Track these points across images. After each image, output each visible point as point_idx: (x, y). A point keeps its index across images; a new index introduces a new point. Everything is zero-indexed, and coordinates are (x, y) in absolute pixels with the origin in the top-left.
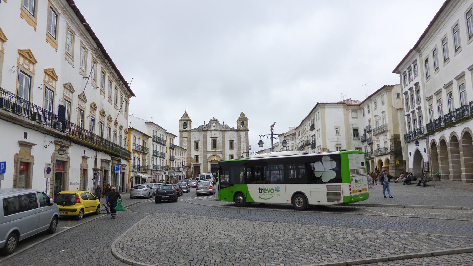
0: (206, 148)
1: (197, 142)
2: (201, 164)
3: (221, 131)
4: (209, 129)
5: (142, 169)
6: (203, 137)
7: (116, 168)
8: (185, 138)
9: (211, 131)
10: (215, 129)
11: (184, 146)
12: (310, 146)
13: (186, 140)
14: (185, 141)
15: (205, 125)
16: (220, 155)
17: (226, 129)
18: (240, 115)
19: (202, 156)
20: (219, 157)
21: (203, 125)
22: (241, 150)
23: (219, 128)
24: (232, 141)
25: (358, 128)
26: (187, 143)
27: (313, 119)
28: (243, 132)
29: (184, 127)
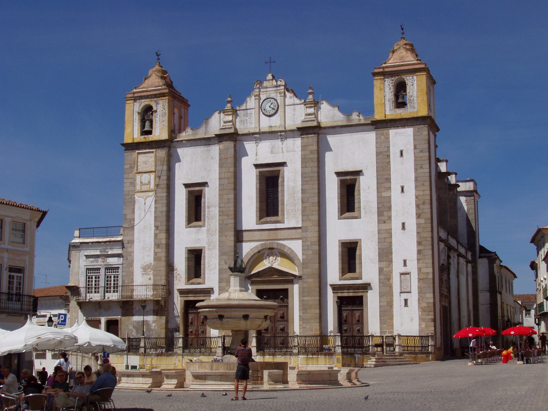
1: (197, 189)
5: (2, 309)
6: (221, 166)
13: (149, 182)
14: (145, 188)
19: (216, 252)
22: (390, 218)
24: (348, 177)
29: (143, 126)
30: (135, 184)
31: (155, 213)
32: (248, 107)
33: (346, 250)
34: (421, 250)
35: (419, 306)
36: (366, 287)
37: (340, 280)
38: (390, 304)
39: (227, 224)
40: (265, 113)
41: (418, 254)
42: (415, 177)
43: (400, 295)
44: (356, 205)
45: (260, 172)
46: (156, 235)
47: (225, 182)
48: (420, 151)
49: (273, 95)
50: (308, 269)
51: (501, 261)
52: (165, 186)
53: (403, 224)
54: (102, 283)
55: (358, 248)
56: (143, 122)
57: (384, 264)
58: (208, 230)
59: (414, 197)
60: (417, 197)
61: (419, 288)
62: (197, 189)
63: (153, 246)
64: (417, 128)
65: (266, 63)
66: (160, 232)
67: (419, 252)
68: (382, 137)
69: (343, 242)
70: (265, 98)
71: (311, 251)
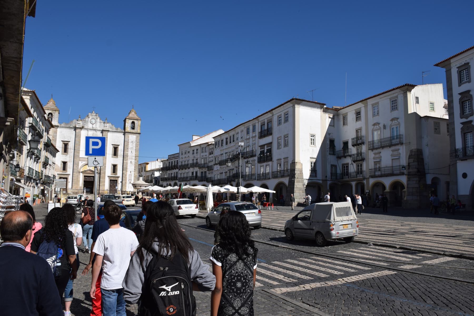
0: (79, 153)
2: (69, 175)
4: (86, 127)
7: (91, 147)
9: (87, 129)
10: (94, 127)
12: (256, 158)
17: (110, 130)
22: (127, 159)
23: (100, 127)
24: (116, 146)
25: (334, 139)
27: (267, 123)
28: (133, 136)
33: (113, 166)
36: (118, 177)
38: (126, 183)
49: (94, 118)
58: (69, 156)
60: (135, 154)
61: (134, 179)
67: (135, 169)
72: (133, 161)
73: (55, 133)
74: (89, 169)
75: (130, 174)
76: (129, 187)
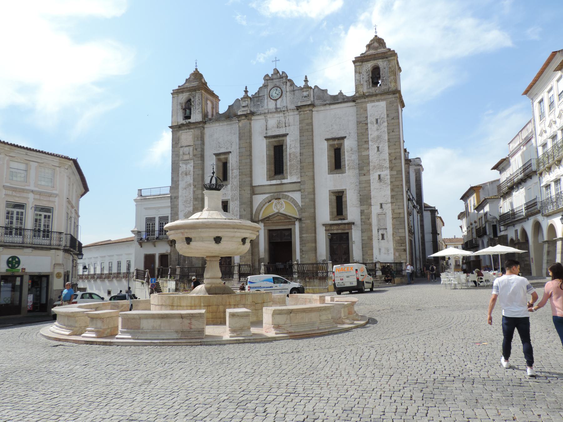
3: (298, 108)
6: (240, 139)
8: (187, 148)
10: (278, 106)
11: (182, 172)
13: (189, 153)
14: (186, 157)
15: (246, 97)
16: (297, 196)
18: (369, 46)
19: (237, 203)
20: (294, 201)
21: (242, 99)
22: (369, 171)
26: (192, 164)
28: (377, 104)
30: (179, 155)
31: (193, 175)
32: (260, 95)
33: (334, 198)
34: (394, 195)
35: (393, 239)
37: (330, 220)
38: (370, 239)
39: (245, 181)
40: (272, 98)
41: (391, 198)
42: (388, 139)
43: (378, 231)
44: (342, 164)
45: (269, 142)
46: (194, 192)
47: (243, 150)
48: (392, 119)
49: (278, 84)
50: (306, 213)
51: (438, 214)
52: (200, 156)
53: (379, 176)
54: (157, 228)
55: (344, 196)
56: (185, 110)
57: (364, 207)
58: (232, 187)
59: (388, 154)
60: (390, 154)
61: (393, 225)
62: (222, 157)
63: (192, 199)
64: (389, 101)
65: (273, 61)
66: (197, 190)
67: (392, 197)
68: (362, 110)
69: (332, 191)
70: (273, 87)
71: (308, 199)
72: (386, 173)
73: (198, 140)
74: (276, 211)
75: (380, 211)
76: (380, 249)
